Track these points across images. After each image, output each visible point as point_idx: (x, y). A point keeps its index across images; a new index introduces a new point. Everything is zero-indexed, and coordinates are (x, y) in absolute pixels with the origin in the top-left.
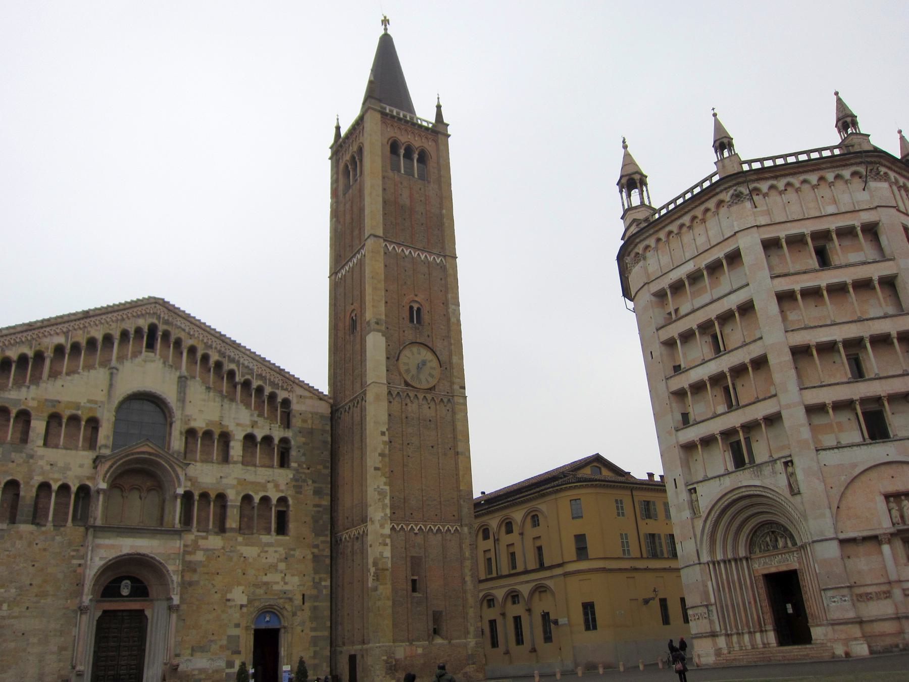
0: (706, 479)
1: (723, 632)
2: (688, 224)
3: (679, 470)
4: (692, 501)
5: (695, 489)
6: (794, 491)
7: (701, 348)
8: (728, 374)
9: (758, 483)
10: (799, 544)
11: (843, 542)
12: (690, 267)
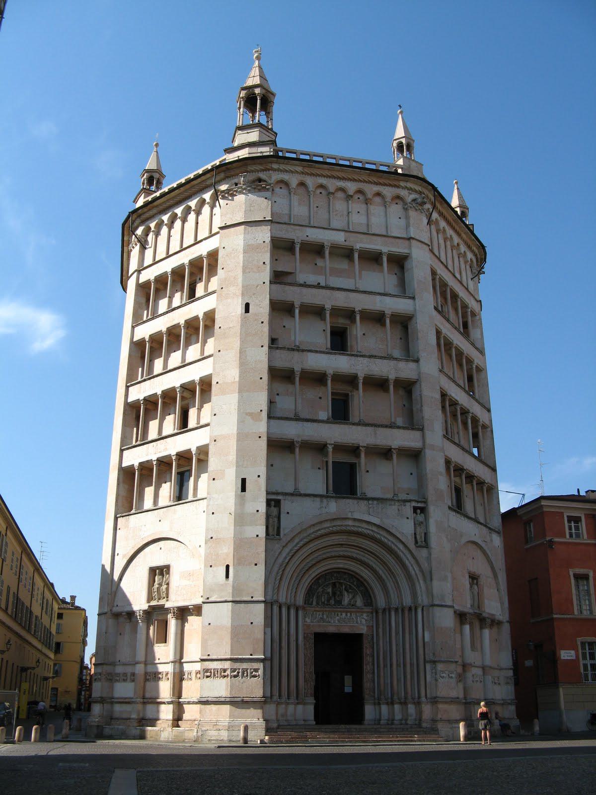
0: (296, 494)
1: (276, 698)
2: (351, 193)
3: (262, 470)
4: (268, 516)
5: (278, 503)
6: (423, 542)
7: (317, 334)
8: (361, 381)
9: (376, 521)
10: (381, 602)
11: (455, 612)
12: (339, 238)
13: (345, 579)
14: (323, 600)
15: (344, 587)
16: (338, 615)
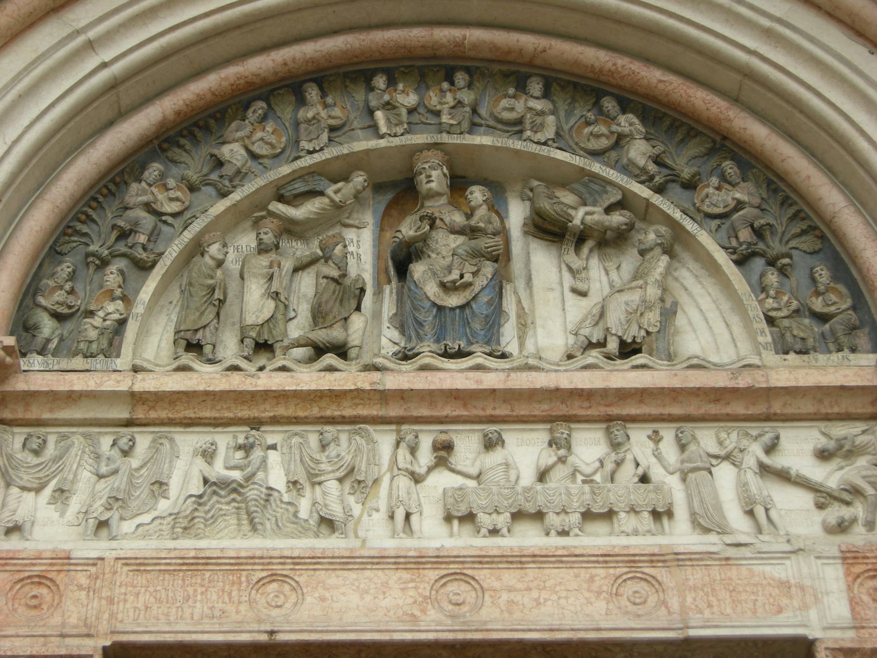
13: (516, 127)
14: (255, 304)
15: (517, 214)
16: (443, 450)
